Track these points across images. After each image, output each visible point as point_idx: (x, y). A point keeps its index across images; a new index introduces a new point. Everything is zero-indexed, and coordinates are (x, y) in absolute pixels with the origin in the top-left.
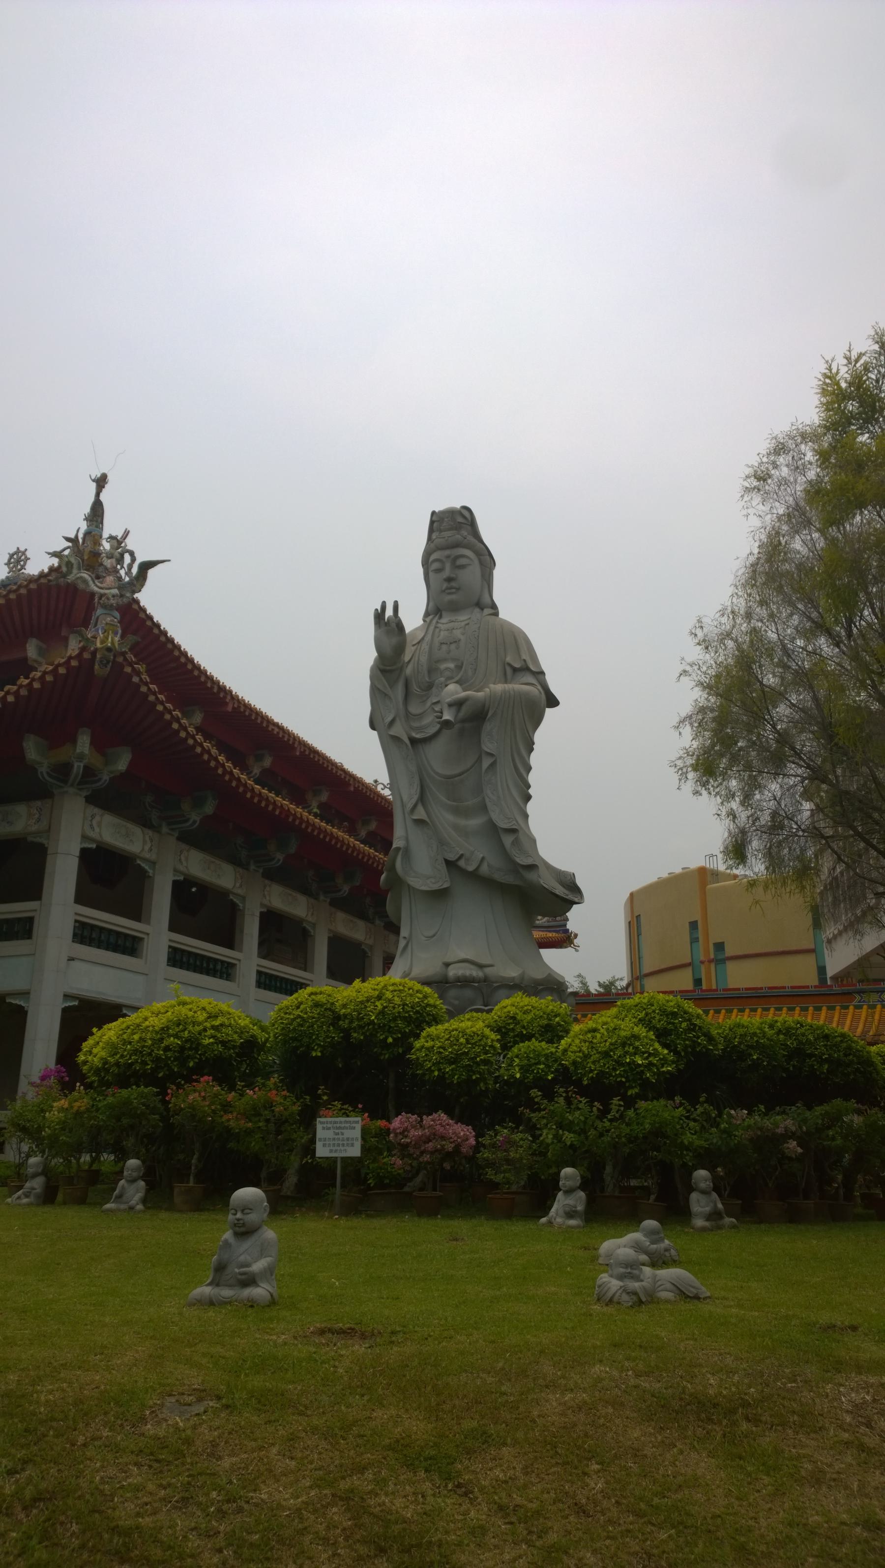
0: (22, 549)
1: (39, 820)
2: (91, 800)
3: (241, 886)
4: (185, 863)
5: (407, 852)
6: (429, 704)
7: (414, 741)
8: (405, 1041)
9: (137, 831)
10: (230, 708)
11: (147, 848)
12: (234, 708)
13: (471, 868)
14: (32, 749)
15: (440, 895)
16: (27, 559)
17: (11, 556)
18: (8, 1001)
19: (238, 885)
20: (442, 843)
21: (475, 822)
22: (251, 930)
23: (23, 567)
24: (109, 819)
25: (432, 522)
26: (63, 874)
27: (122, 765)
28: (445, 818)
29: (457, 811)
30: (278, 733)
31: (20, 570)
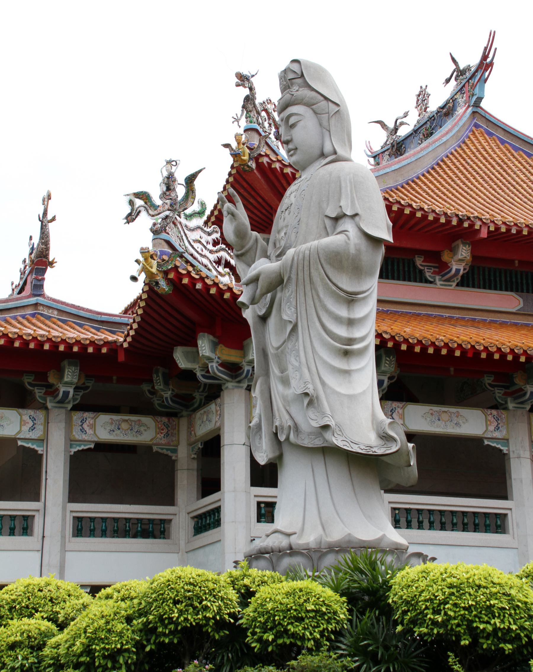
3: (497, 428)
12: (489, 232)
16: (429, 95)
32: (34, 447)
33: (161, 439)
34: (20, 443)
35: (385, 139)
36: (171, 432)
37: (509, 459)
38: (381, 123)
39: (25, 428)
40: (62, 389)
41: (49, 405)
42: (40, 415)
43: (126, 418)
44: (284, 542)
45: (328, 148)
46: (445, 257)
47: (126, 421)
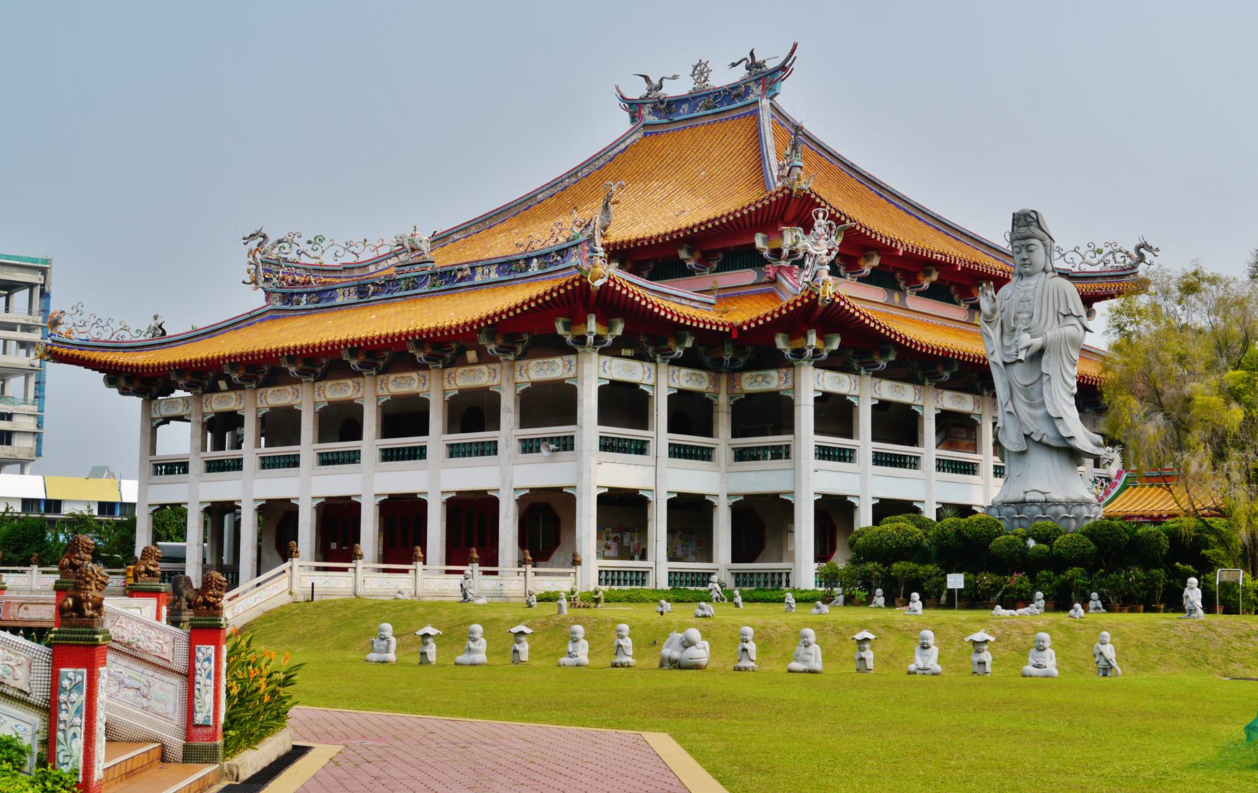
0: (704, 61)
2: (817, 365)
7: (1005, 364)
8: (991, 539)
13: (1037, 439)
14: (781, 343)
15: (1022, 453)
20: (1021, 424)
21: (1039, 412)
22: (929, 429)
24: (829, 375)
26: (805, 415)
27: (835, 345)
28: (1023, 410)
29: (1030, 406)
36: (715, 382)
38: (647, 78)
41: (658, 360)
42: (652, 366)
44: (1042, 498)
45: (1049, 268)
46: (861, 262)
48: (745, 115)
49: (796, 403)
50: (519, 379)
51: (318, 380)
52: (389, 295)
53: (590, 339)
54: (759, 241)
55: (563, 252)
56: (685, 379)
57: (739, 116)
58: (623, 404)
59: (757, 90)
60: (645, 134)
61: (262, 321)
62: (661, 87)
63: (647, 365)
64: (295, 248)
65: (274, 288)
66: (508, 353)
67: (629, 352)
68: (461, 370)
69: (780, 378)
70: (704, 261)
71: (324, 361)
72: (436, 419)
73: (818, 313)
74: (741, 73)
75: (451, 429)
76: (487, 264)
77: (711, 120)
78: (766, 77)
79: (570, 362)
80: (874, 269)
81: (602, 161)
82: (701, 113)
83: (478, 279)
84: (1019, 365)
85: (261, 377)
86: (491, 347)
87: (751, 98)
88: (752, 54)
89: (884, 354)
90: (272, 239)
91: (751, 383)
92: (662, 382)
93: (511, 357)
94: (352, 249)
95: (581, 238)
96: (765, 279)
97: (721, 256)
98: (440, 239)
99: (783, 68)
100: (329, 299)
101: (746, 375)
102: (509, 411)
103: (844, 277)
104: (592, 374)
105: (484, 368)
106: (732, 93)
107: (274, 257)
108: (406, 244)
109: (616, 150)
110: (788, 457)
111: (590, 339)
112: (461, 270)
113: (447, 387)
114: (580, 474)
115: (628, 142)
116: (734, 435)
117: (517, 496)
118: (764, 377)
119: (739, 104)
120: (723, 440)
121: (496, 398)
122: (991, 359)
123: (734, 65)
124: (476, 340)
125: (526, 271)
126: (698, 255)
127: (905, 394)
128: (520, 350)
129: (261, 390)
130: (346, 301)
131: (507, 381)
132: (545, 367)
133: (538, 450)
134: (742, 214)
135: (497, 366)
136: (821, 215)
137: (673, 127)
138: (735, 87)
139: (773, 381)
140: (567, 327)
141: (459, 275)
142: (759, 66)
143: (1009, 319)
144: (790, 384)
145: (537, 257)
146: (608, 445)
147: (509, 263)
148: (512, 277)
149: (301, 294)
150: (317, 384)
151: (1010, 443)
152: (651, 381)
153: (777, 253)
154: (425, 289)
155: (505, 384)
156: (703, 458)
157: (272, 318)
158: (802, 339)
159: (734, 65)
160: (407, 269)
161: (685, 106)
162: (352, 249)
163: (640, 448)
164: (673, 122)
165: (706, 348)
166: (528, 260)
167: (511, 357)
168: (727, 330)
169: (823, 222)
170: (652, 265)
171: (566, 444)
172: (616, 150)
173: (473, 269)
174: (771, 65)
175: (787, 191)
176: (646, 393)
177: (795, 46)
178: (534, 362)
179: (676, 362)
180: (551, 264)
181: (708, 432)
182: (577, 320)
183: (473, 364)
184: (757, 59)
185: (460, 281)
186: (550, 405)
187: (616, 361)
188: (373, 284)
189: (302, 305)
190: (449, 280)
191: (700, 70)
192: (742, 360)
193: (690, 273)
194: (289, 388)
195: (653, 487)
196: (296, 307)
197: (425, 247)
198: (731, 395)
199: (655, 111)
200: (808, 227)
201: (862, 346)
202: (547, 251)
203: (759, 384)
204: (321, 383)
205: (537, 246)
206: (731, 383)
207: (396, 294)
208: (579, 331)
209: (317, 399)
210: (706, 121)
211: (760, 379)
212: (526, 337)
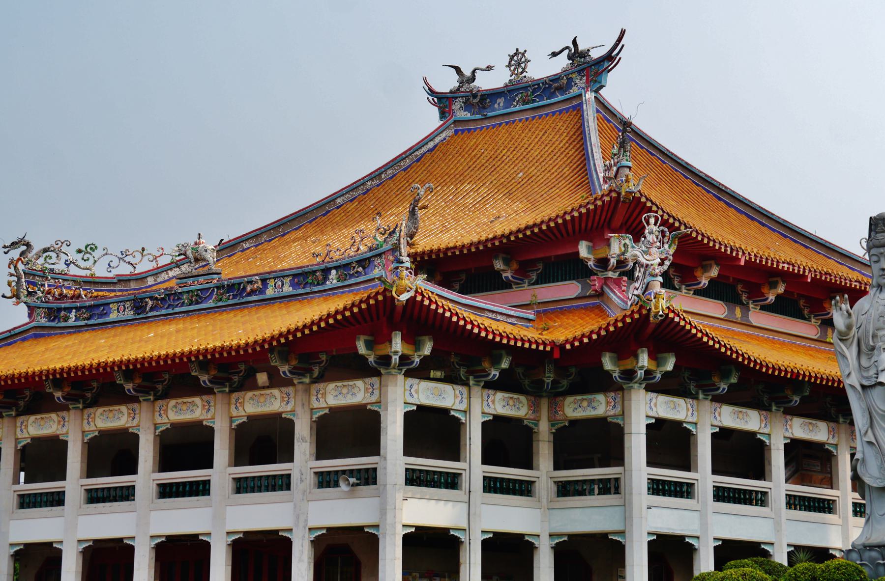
0: (521, 50)
1: (614, 407)
2: (650, 388)
3: (766, 426)
4: (719, 419)
5: (863, 460)
6: (873, 361)
7: (864, 387)
9: (681, 401)
10: (742, 263)
11: (690, 413)
14: (608, 363)
17: (512, 58)
18: (610, 537)
19: (763, 425)
22: (778, 460)
23: (524, 70)
24: (662, 398)
25: (871, 225)
26: (637, 445)
27: (669, 366)
30: (788, 268)
31: (522, 73)
32: (460, 416)
33: (530, 415)
34: (452, 413)
35: (457, 84)
36: (535, 407)
37: (770, 449)
38: (458, 69)
39: (457, 401)
40: (493, 372)
41: (471, 382)
42: (465, 390)
43: (511, 395)
46: (698, 273)
47: (511, 398)
48: (567, 110)
49: (626, 431)
50: (316, 405)
51: (87, 406)
52: (170, 311)
53: (395, 359)
54: (583, 250)
55: (365, 262)
56: (501, 404)
57: (561, 112)
58: (432, 432)
59: (580, 82)
60: (456, 132)
61: (24, 339)
62: (473, 78)
63: (458, 388)
64: (63, 257)
65: (38, 303)
66: (303, 375)
67: (438, 374)
68: (250, 394)
69: (608, 403)
70: (522, 273)
71: (95, 384)
72: (222, 451)
73: (650, 329)
74: (562, 63)
75: (238, 459)
76: (280, 275)
77: (529, 115)
78: (590, 68)
79: (372, 385)
80: (712, 281)
81: (408, 162)
82: (518, 108)
83: (270, 292)
84: (879, 389)
85: (22, 403)
86: (284, 369)
87: (574, 91)
88: (574, 42)
89: (725, 376)
90: (37, 247)
91: (576, 409)
92: (475, 408)
93: (307, 380)
94: (128, 259)
95: (386, 247)
96: (590, 292)
97: (541, 266)
98: (227, 248)
99: (610, 58)
100: (101, 315)
101: (570, 399)
102: (303, 440)
103: (679, 290)
104: (398, 400)
105: (276, 392)
106: (551, 86)
107: (39, 267)
108: (189, 253)
109: (424, 149)
110: (617, 491)
111: (395, 359)
112: (251, 282)
113: (234, 413)
114: (383, 512)
115: (437, 140)
116: (557, 467)
117: (312, 537)
118: (590, 402)
119: (560, 98)
120: (544, 472)
121: (289, 426)
122: (847, 382)
123: (554, 54)
124: (267, 360)
125: (324, 283)
126: (515, 266)
127: (750, 421)
128: (316, 373)
129: (22, 418)
130: (121, 317)
131: (301, 407)
132: (345, 391)
133: (337, 485)
134: (564, 220)
135: (290, 390)
136: (652, 221)
137: (487, 123)
138: (556, 79)
139: (599, 406)
140: (369, 345)
141: (249, 288)
142: (584, 54)
143: (867, 337)
144: (618, 410)
145: (336, 268)
146: (414, 478)
147: (305, 274)
148: (308, 290)
149: (69, 310)
150: (86, 411)
151: (871, 477)
152: (463, 407)
153: (603, 263)
154: (210, 303)
155: (299, 410)
156: (521, 493)
157: (36, 336)
158: (632, 358)
159: (554, 54)
160: (190, 281)
161: (501, 101)
162: (128, 259)
163: (451, 481)
164: (487, 118)
165: (526, 369)
166: (326, 271)
167: (307, 380)
168: (548, 348)
169: (655, 228)
170: (463, 277)
171: (368, 477)
172: (424, 149)
173: (264, 281)
174: (595, 54)
175: (614, 195)
176: (458, 419)
177: (623, 33)
178: (332, 386)
179: (492, 385)
180: (352, 276)
181: (528, 463)
182: (380, 338)
183: (264, 388)
184: (582, 47)
185: (249, 294)
186: (350, 433)
187: (424, 384)
188: (151, 298)
189: (71, 322)
190: (238, 295)
191: (517, 60)
192: (565, 383)
193: (506, 285)
194: (54, 416)
195: (465, 526)
196: (63, 324)
197: (211, 257)
198: (552, 422)
199: (468, 106)
200: (638, 234)
201: (700, 368)
202: (344, 262)
203: (584, 410)
204: (92, 410)
205: (336, 256)
206: (554, 408)
207: (177, 310)
208: (383, 350)
209: (87, 428)
210: (524, 116)
211: (585, 404)
212: (324, 357)
